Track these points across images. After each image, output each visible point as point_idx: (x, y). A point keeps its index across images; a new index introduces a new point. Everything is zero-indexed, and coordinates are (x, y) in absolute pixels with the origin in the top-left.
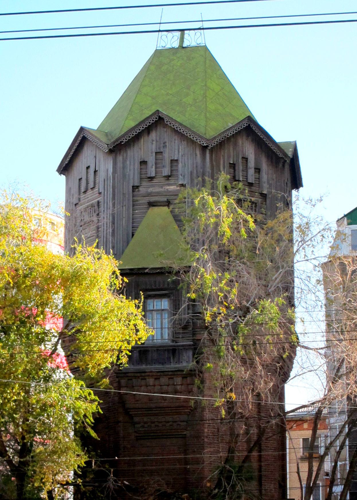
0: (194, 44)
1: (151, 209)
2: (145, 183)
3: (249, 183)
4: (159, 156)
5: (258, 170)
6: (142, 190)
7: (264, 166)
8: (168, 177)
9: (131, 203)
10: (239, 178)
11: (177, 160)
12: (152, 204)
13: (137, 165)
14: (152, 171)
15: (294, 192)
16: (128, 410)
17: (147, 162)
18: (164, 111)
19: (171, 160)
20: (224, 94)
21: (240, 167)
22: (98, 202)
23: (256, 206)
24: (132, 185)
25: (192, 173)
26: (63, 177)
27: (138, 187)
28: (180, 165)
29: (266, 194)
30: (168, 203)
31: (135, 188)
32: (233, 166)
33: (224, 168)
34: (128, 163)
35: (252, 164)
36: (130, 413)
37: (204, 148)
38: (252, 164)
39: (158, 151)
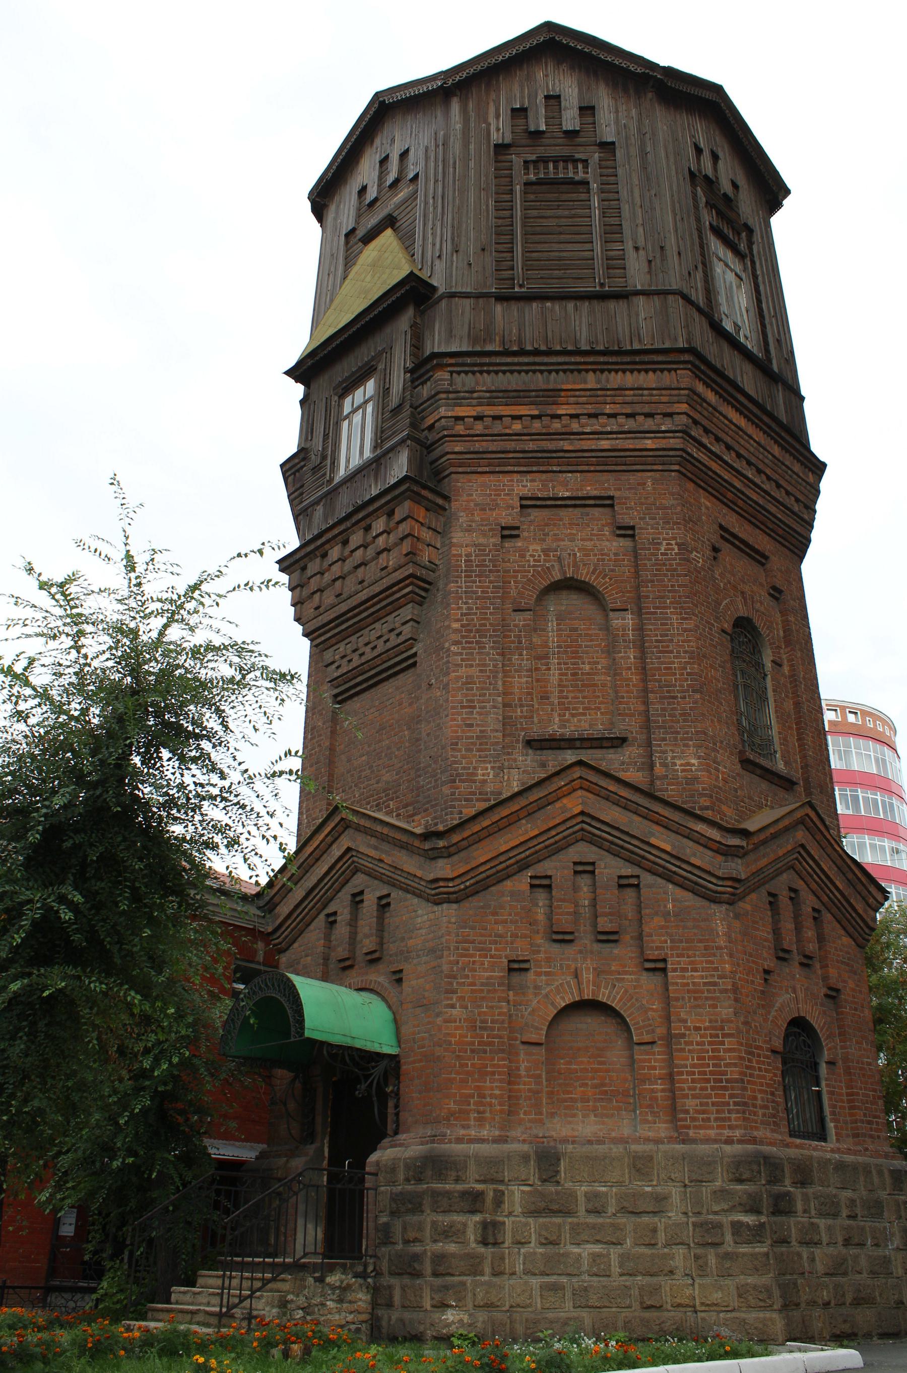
3: (567, 132)
10: (538, 125)
23: (586, 167)
29: (613, 143)
33: (497, 116)
34: (342, 206)
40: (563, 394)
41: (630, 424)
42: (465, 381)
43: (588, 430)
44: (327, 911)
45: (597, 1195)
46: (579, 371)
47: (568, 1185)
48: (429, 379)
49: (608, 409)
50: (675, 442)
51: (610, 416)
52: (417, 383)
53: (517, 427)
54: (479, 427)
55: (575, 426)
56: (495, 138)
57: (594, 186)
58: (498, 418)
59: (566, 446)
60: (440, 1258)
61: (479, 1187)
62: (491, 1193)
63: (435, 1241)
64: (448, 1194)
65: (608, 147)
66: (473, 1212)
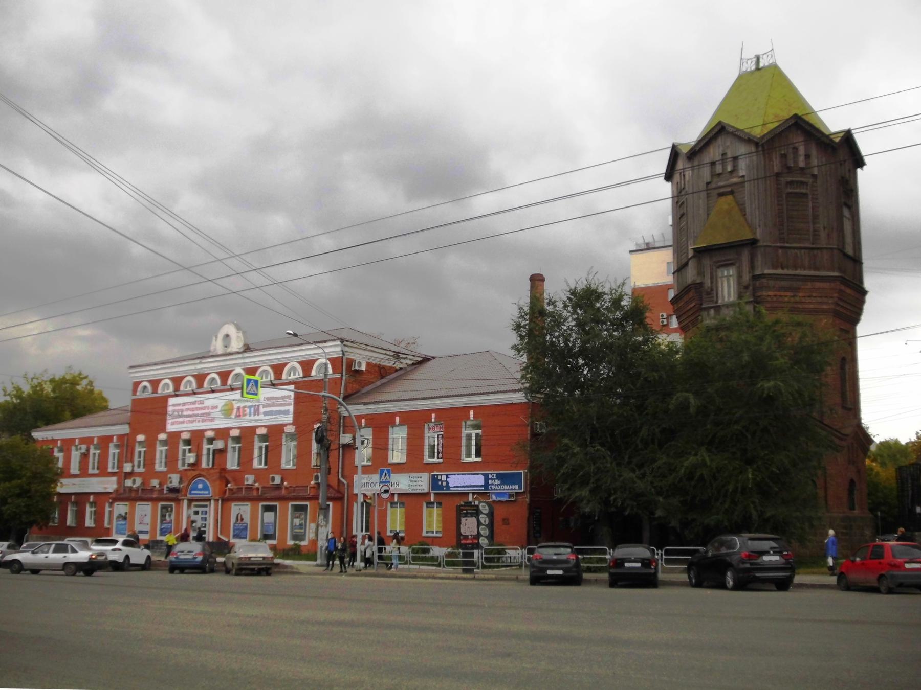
0: (767, 64)
2: (715, 180)
5: (807, 157)
6: (713, 185)
7: (814, 152)
8: (731, 172)
12: (721, 195)
14: (719, 169)
15: (859, 170)
18: (728, 120)
20: (785, 100)
21: (791, 156)
22: (686, 199)
23: (807, 185)
24: (705, 181)
26: (669, 184)
30: (732, 193)
31: (708, 184)
32: (784, 156)
35: (802, 150)
37: (757, 144)
38: (802, 150)
41: (819, 300)
42: (771, 283)
43: (807, 301)
49: (814, 295)
50: (832, 306)
51: (815, 297)
54: (775, 299)
55: (803, 300)
56: (776, 169)
57: (810, 197)
58: (781, 296)
59: (800, 306)
65: (814, 176)
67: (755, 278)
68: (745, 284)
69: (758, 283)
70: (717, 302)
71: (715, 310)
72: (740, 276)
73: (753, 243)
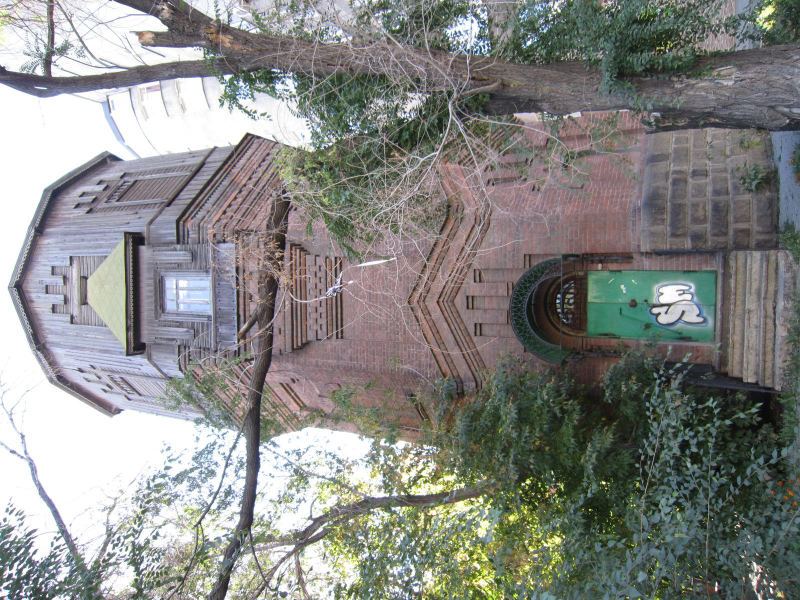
1: (89, 302)
4: (50, 289)
9: (83, 326)
11: (53, 268)
13: (55, 317)
16: (295, 347)
17: (53, 305)
19: (53, 274)
24: (69, 325)
25: (62, 249)
27: (72, 317)
28: (56, 264)
34: (53, 328)
36: (300, 344)
39: (45, 290)
40: (236, 180)
44: (472, 334)
45: (677, 139)
46: (228, 173)
47: (671, 151)
48: (188, 232)
52: (186, 241)
53: (240, 200)
60: (716, 192)
61: (670, 180)
62: (675, 176)
63: (705, 195)
64: (674, 192)
66: (686, 181)
67: (181, 238)
68: (188, 257)
69: (193, 235)
70: (209, 317)
71: (221, 323)
72: (178, 267)
73: (136, 240)
